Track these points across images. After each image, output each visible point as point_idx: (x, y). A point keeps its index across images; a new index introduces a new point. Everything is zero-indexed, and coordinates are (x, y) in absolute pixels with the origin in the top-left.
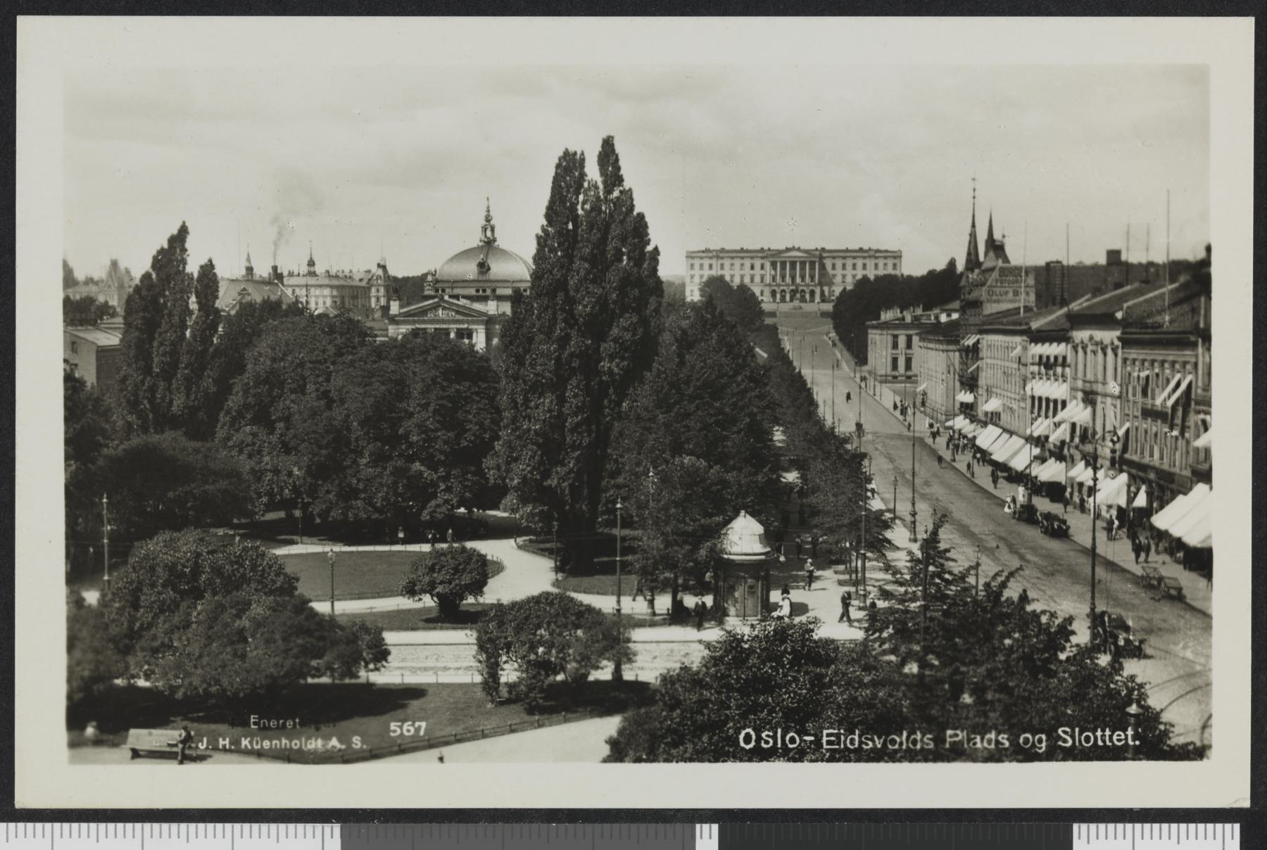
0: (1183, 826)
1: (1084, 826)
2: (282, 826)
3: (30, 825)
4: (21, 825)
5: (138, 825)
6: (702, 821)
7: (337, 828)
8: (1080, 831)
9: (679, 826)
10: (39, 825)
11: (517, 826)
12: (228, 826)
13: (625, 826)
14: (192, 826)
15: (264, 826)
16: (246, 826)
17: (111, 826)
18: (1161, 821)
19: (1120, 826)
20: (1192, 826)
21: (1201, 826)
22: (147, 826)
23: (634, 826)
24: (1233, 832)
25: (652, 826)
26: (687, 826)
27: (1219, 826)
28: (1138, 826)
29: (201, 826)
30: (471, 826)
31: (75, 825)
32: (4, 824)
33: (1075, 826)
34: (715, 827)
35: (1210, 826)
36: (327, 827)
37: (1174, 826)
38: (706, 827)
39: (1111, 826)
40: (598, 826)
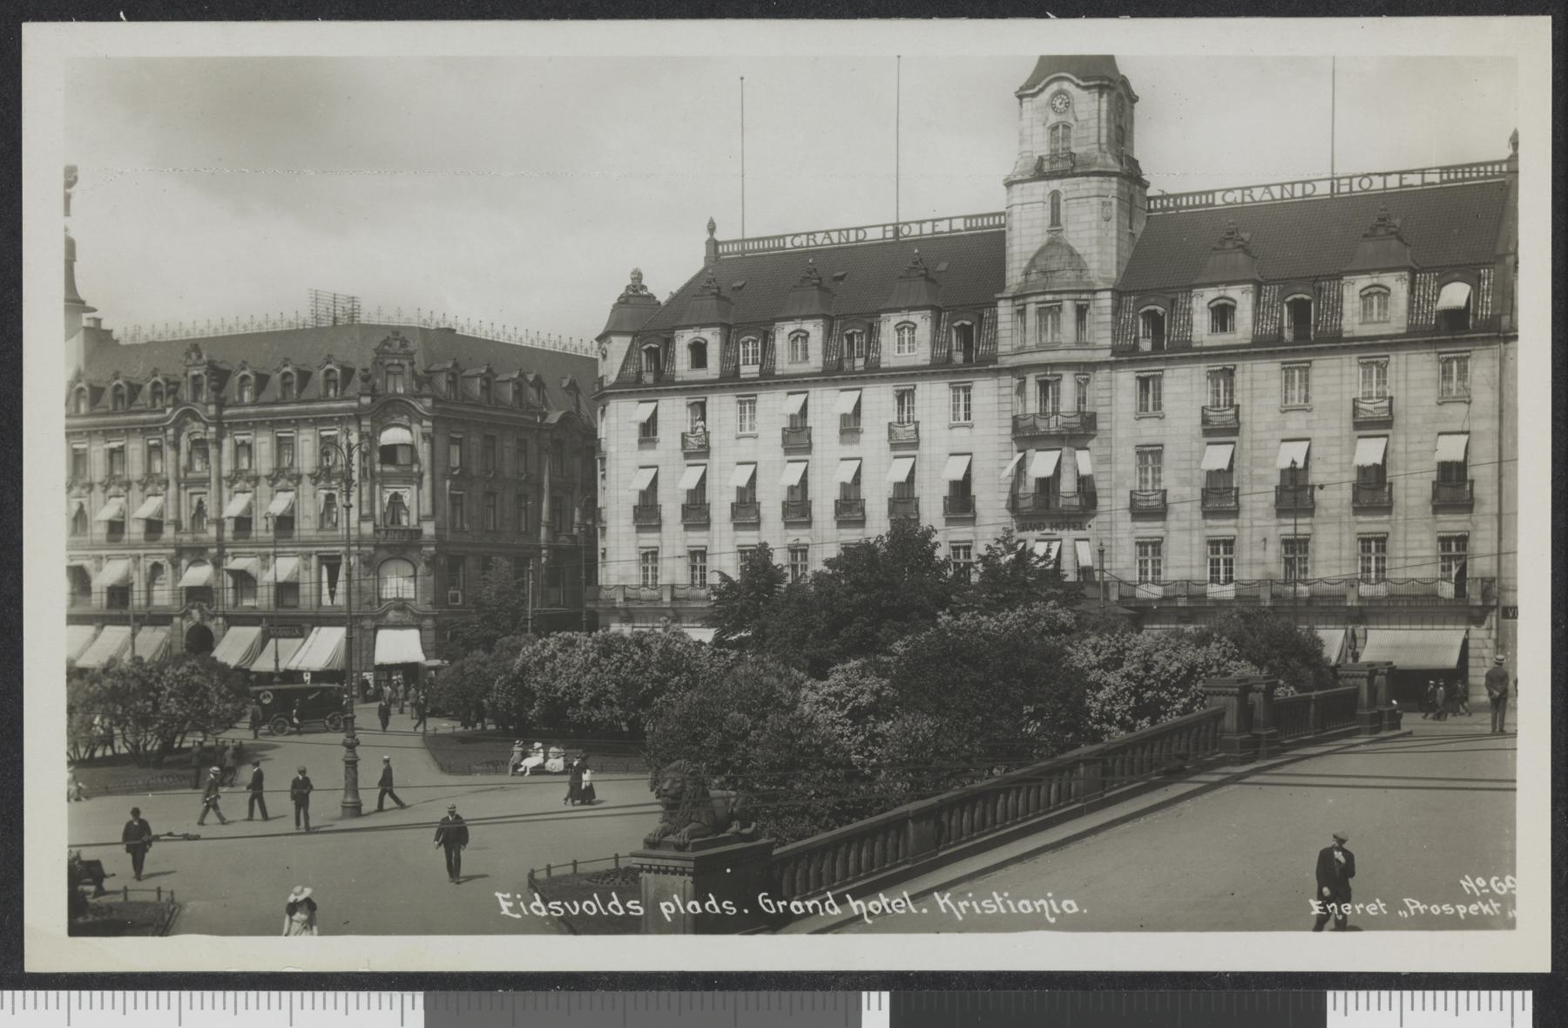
0: (1463, 994)
1: (1340, 994)
2: (352, 995)
3: (41, 994)
4: (30, 993)
5: (174, 994)
6: (869, 989)
7: (419, 996)
8: (1335, 999)
9: (841, 994)
10: (52, 994)
11: (641, 995)
12: (285, 994)
13: (774, 994)
14: (241, 994)
15: (330, 995)
16: (308, 994)
17: (141, 994)
18: (1435, 988)
19: (1385, 994)
20: (1474, 994)
21: (1485, 994)
22: (185, 994)
23: (786, 995)
24: (1522, 1003)
25: (808, 994)
26: (851, 994)
27: (1507, 994)
28: (1407, 994)
29: (252, 994)
30: (585, 995)
31: (97, 994)
32: (7, 994)
33: (1330, 994)
34: (886, 995)
35: (1496, 994)
36: (408, 995)
37: (1451, 994)
38: (874, 995)
39: (1374, 994)
40: (741, 994)
